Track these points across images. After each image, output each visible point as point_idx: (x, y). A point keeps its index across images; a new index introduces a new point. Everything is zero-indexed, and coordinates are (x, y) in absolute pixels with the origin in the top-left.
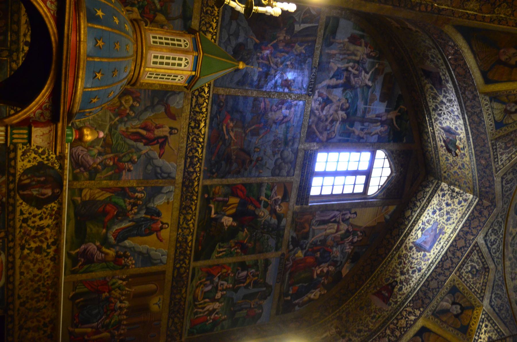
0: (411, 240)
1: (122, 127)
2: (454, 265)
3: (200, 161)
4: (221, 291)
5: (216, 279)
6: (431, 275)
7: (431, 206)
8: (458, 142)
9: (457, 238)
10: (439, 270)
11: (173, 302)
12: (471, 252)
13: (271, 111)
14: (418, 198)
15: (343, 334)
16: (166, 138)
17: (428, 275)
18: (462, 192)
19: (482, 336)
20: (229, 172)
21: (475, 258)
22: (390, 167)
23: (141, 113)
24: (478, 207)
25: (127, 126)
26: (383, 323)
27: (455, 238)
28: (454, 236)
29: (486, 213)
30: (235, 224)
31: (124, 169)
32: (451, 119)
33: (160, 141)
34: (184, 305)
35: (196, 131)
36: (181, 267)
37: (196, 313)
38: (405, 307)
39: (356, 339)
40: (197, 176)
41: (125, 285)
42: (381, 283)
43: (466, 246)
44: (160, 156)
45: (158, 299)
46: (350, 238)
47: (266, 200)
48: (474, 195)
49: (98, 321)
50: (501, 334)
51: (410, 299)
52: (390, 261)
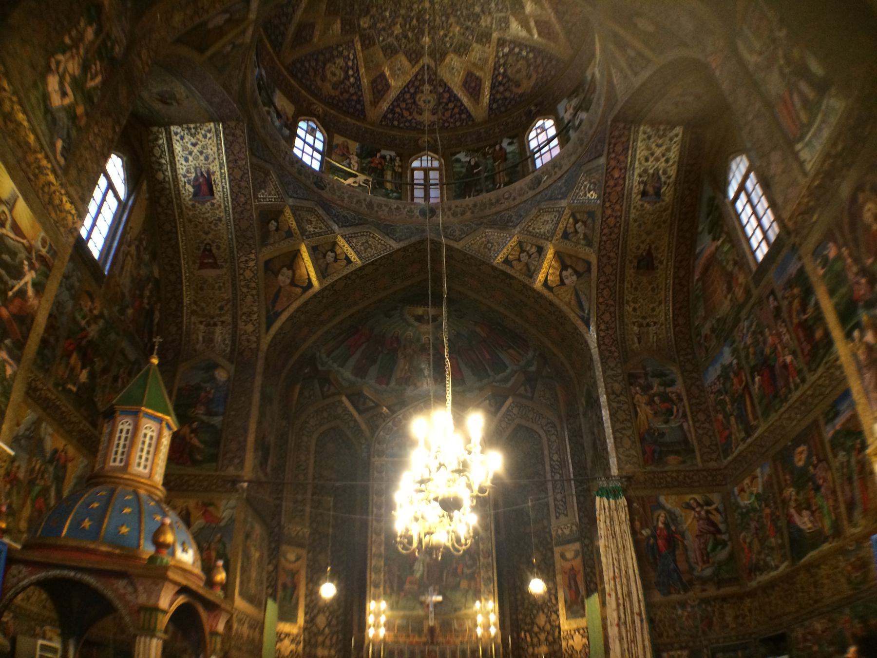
0: (187, 199)
2: (248, 196)
6: (234, 218)
10: (239, 209)
14: (158, 155)
15: (212, 322)
24: (227, 132)
28: (225, 170)
29: (238, 132)
30: (88, 368)
43: (245, 173)
46: (142, 249)
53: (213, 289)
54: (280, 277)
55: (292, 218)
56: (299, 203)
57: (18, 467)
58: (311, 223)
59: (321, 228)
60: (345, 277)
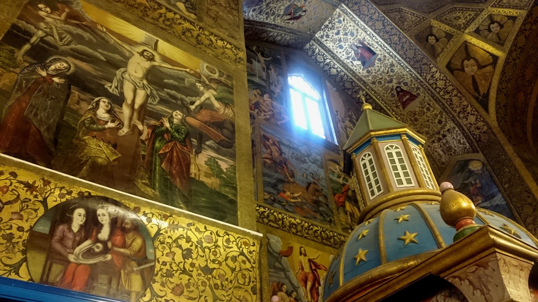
0: (361, 71)
2: (398, 33)
3: (324, 229)
7: (333, 49)
8: (299, 4)
9: (373, 28)
10: (399, 47)
12: (389, 18)
13: (272, 155)
14: (322, 60)
15: (441, 137)
16: (310, 261)
17: (400, 58)
18: (330, 19)
19: (454, 23)
20: (327, 206)
21: (392, 15)
22: (297, 76)
23: (292, 284)
26: (436, 100)
27: (372, 29)
32: (282, 2)
33: (314, 268)
35: (299, 228)
38: (426, 80)
39: (448, 125)
42: (394, 102)
43: (383, 21)
47: (342, 178)
48: (338, 7)
50: (452, 10)
51: (418, 76)
52: (375, 92)
53: (424, 113)
54: (466, 69)
55: (442, 25)
56: (439, 12)
58: (460, 18)
59: (470, 15)
60: (521, 31)
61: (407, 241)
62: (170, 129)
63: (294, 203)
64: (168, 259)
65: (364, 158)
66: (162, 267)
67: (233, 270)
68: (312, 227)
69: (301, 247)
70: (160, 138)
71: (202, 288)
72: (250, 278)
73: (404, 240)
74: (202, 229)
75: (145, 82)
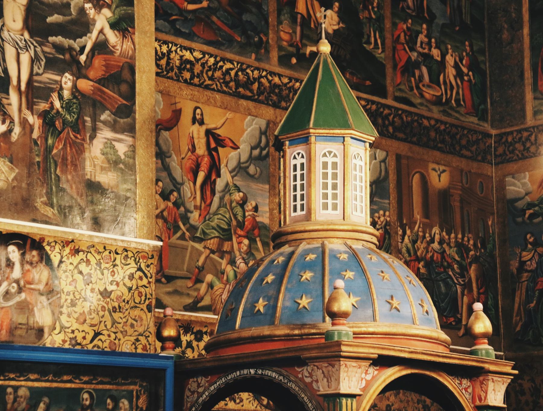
1: (195, 217)
3: (244, 66)
4: (430, 50)
5: (414, 55)
11: (439, 145)
23: (173, 179)
25: (192, 208)
31: (254, 217)
33: (213, 145)
34: (445, 123)
35: (198, 69)
36: (392, 123)
37: (457, 101)
40: (266, 76)
41: (411, 232)
44: (236, 147)
45: (434, 172)
49: (455, 284)
57: (256, 209)
61: (301, 306)
62: (60, 110)
63: (194, 11)
64: (71, 288)
65: (297, 156)
66: (67, 297)
67: (130, 289)
68: (221, 63)
69: (196, 108)
70: (52, 129)
71: (101, 313)
72: (146, 296)
73: (299, 304)
74: (101, 250)
75: (27, 35)
